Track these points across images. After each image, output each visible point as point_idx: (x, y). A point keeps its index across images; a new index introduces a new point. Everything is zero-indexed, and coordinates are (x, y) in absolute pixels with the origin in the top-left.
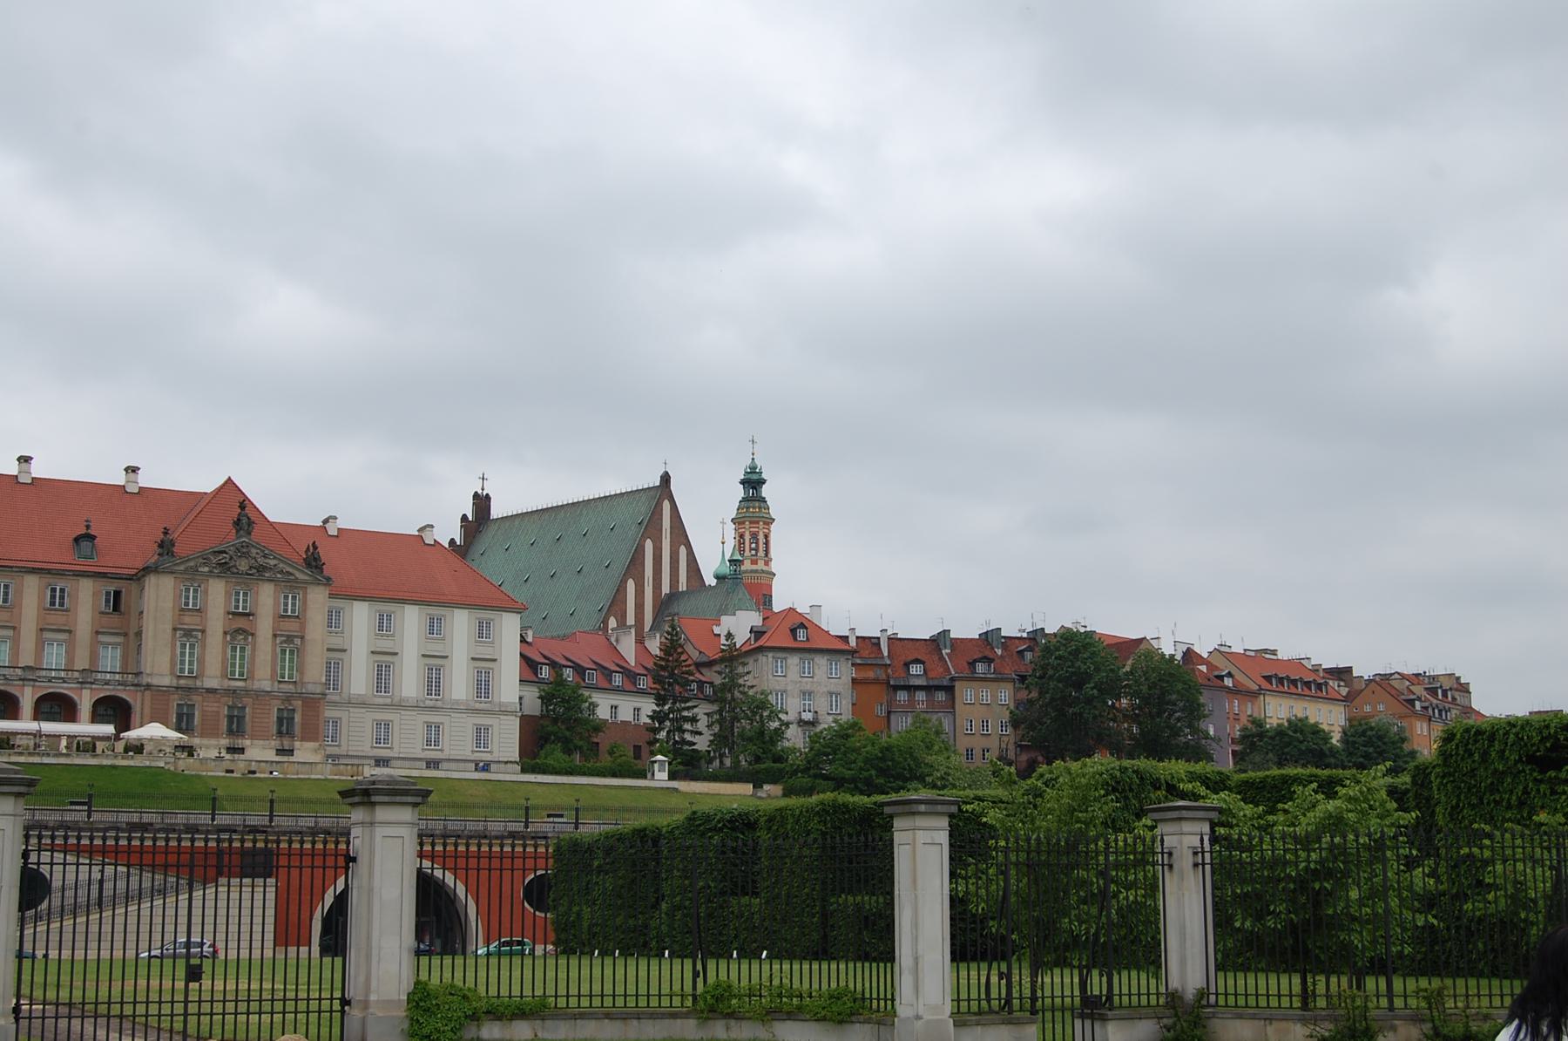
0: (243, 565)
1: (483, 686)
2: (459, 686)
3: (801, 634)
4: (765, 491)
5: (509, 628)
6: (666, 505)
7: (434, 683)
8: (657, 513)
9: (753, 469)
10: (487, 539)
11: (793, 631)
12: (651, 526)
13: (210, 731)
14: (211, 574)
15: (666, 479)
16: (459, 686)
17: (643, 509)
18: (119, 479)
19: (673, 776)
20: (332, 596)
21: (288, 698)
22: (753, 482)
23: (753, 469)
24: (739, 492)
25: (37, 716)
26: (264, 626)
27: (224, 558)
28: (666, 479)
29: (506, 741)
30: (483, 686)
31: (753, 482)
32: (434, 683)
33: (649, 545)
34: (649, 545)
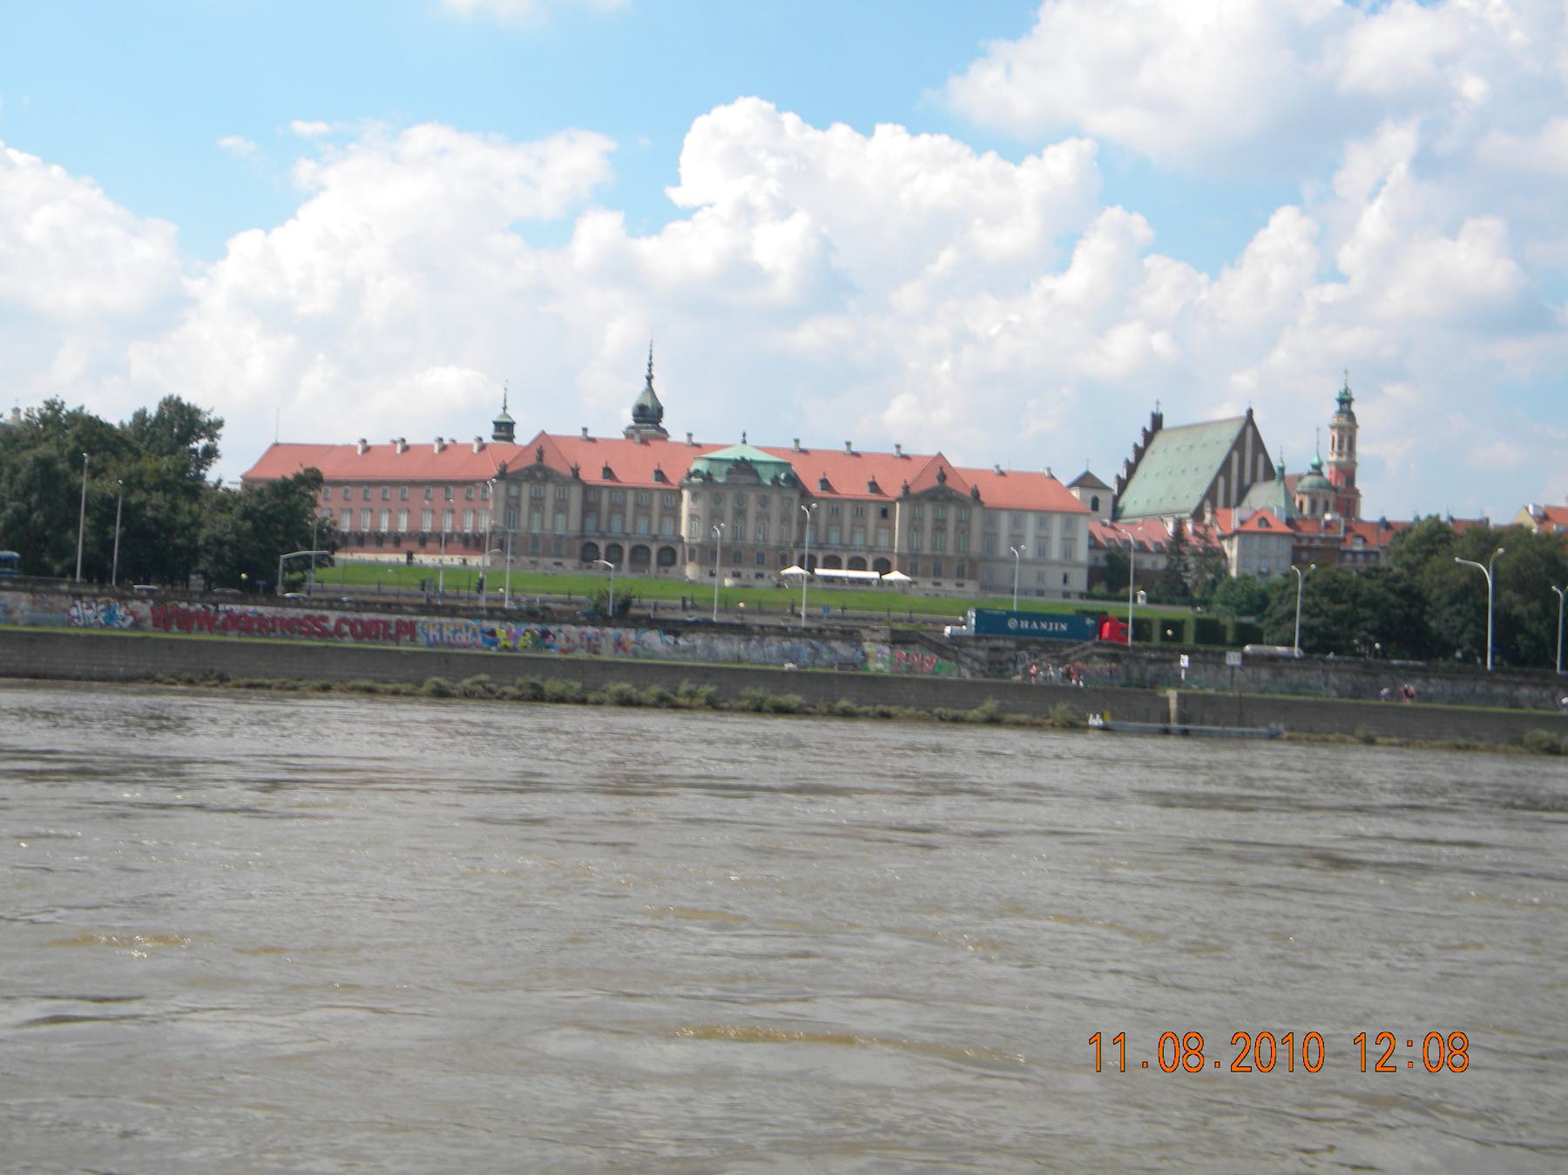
1: (1068, 552)
2: (1055, 552)
7: (1042, 550)
9: (1346, 392)
10: (1159, 440)
13: (925, 575)
15: (1250, 412)
16: (1055, 552)
17: (1232, 433)
19: (1150, 601)
21: (962, 560)
22: (1345, 401)
23: (1346, 392)
24: (1337, 407)
25: (850, 568)
26: (951, 526)
28: (1250, 412)
29: (1079, 581)
30: (1068, 552)
31: (1345, 401)
32: (1042, 550)
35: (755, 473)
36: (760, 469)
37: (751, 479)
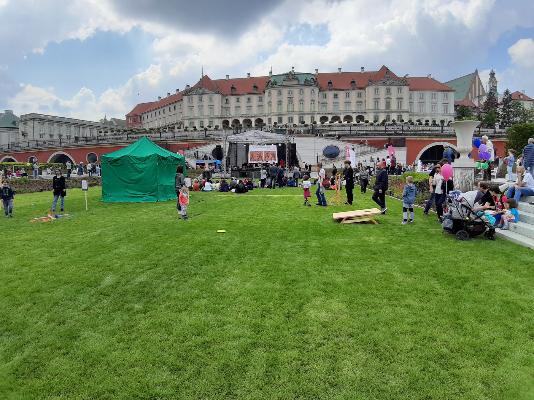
0: (388, 83)
3: (522, 97)
4: (495, 76)
5: (451, 95)
6: (477, 77)
8: (475, 78)
9: (492, 71)
11: (519, 96)
12: (474, 82)
14: (381, 85)
15: (477, 71)
18: (360, 70)
20: (410, 90)
22: (492, 74)
23: (492, 71)
24: (489, 76)
27: (384, 81)
28: (477, 71)
31: (492, 74)
33: (473, 85)
34: (473, 85)
35: (298, 80)
36: (299, 77)
37: (295, 82)
